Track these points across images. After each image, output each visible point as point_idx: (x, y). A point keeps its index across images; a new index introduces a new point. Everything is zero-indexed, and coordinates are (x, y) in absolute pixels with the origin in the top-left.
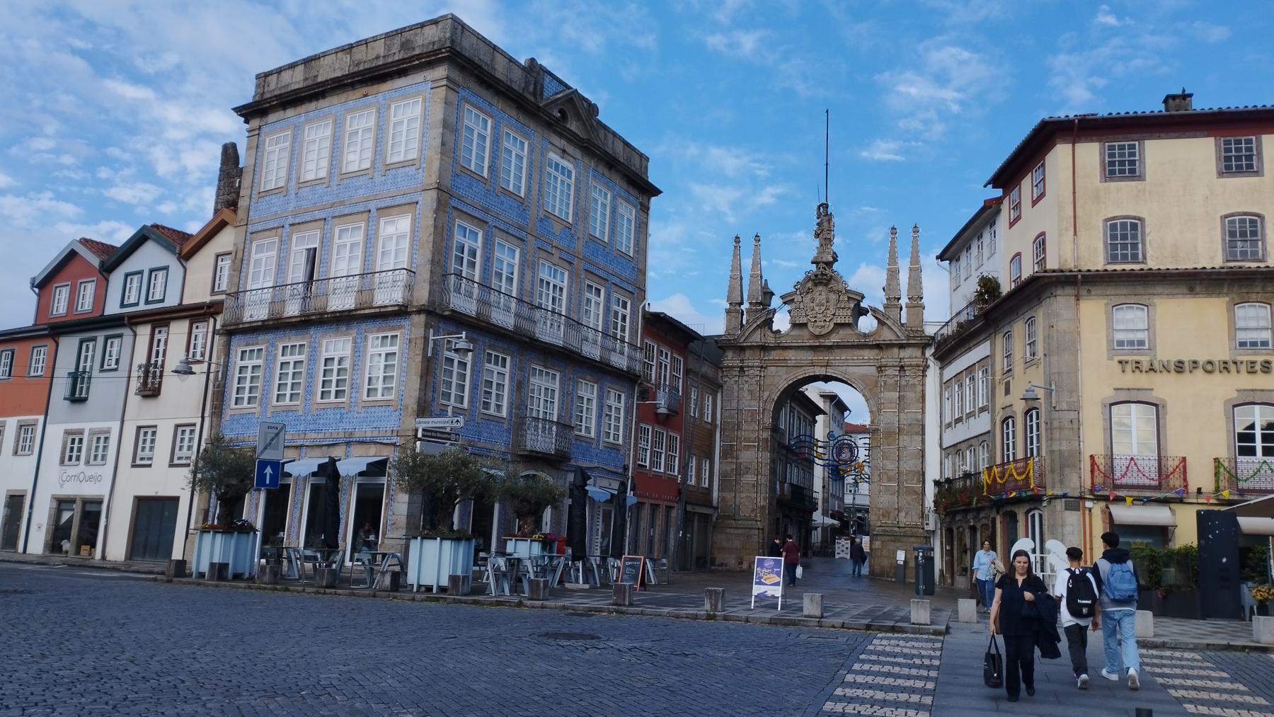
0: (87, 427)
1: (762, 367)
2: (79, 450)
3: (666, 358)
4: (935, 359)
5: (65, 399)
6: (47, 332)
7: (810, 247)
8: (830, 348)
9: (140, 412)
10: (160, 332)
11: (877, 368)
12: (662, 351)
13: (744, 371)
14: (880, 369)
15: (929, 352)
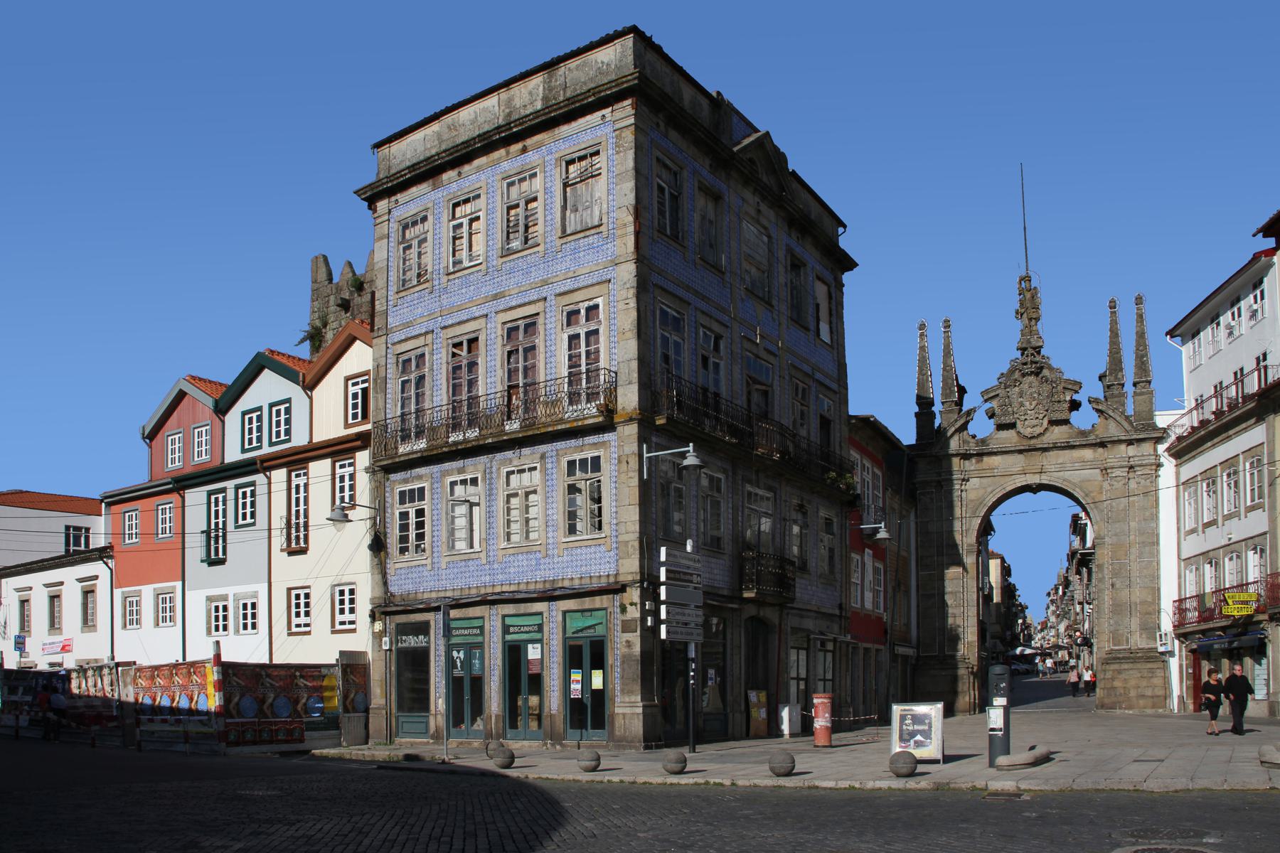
0: (230, 591)
1: (963, 480)
2: (225, 618)
3: (868, 473)
4: (1171, 455)
5: (202, 561)
6: (171, 486)
7: (1013, 331)
8: (1045, 450)
9: (289, 571)
10: (298, 476)
11: (1102, 471)
12: (864, 465)
13: (942, 487)
14: (1105, 470)
15: (1161, 448)
